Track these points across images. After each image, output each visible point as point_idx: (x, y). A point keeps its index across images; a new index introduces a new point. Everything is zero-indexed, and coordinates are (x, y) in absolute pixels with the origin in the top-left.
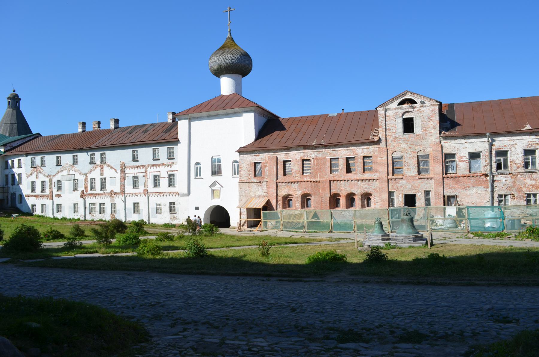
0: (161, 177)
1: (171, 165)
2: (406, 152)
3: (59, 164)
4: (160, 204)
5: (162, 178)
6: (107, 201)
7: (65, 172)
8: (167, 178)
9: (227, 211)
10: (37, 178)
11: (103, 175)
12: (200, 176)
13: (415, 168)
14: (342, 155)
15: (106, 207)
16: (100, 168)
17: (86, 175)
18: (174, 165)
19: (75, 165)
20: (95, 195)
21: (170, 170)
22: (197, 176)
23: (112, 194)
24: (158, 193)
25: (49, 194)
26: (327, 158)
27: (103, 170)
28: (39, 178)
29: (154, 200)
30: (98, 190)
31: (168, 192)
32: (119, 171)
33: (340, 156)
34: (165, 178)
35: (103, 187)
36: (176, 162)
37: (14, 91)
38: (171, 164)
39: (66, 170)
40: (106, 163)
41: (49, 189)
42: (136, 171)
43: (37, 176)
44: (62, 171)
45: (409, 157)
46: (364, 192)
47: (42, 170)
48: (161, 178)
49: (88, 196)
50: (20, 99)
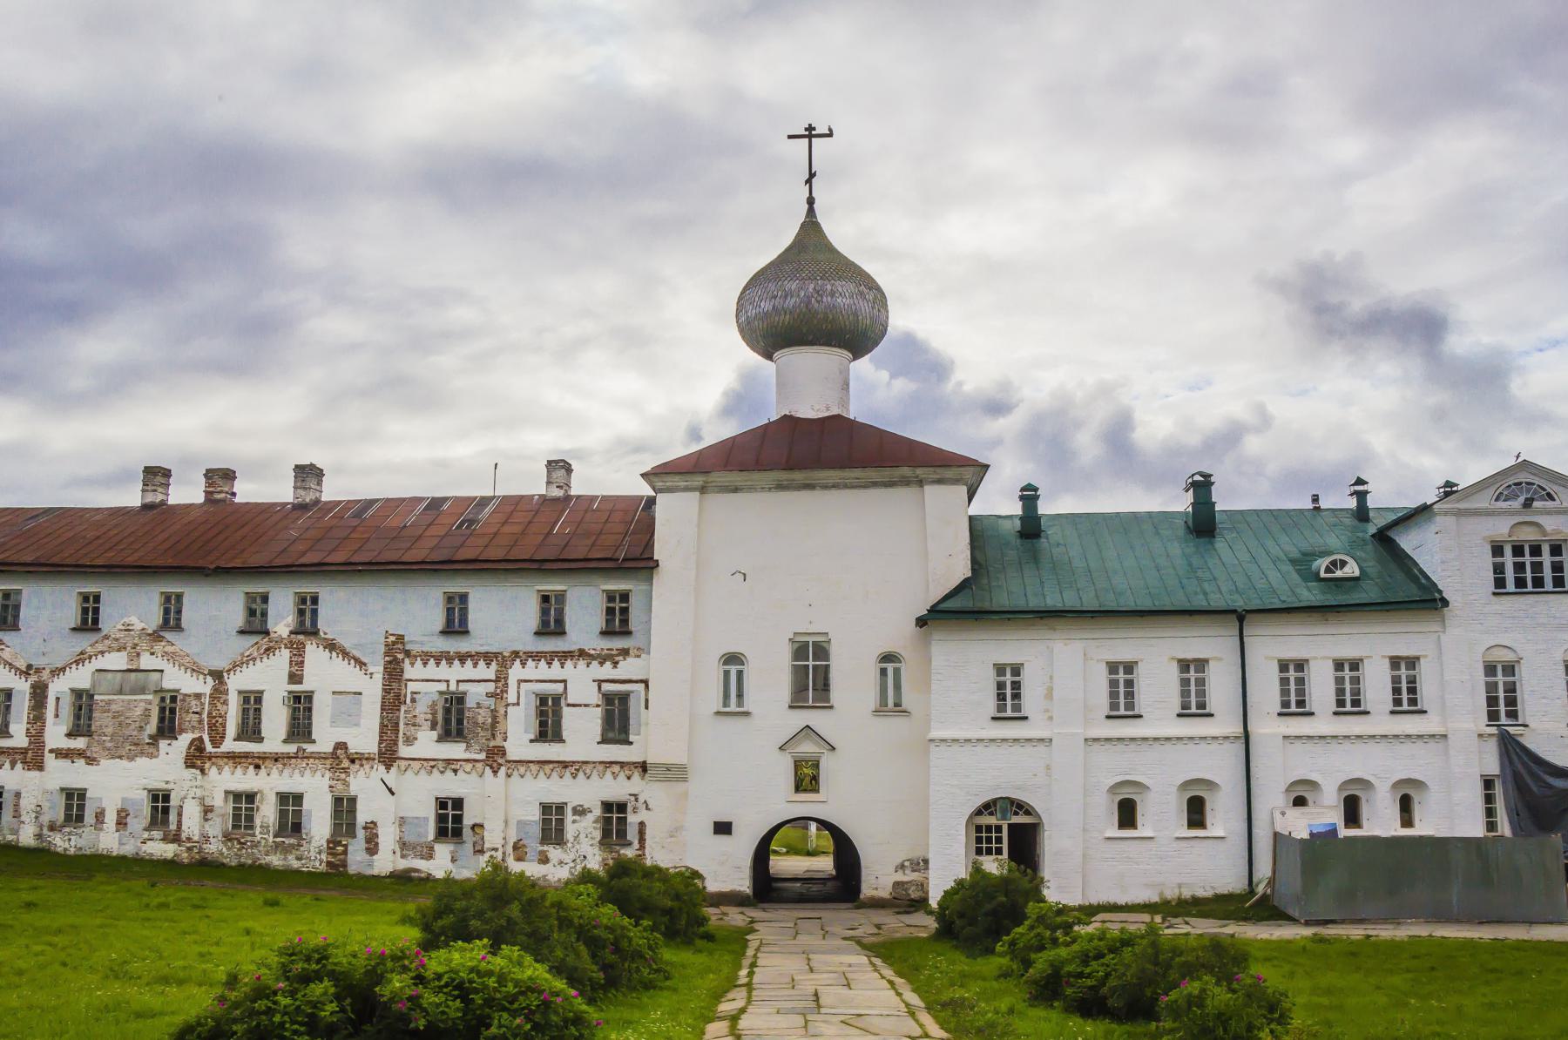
0: (570, 701)
1: (617, 658)
3: (89, 621)
4: (560, 808)
5: (574, 705)
7: (117, 661)
8: (598, 706)
11: (301, 683)
12: (740, 704)
15: (310, 812)
16: (288, 650)
17: (217, 675)
18: (630, 660)
19: (168, 635)
20: (257, 762)
21: (611, 677)
23: (341, 759)
27: (302, 662)
32: (378, 670)
34: (586, 706)
35: (300, 728)
36: (638, 649)
38: (617, 655)
39: (119, 650)
40: (314, 633)
41: (24, 726)
42: (454, 673)
48: (569, 705)
49: (221, 762)
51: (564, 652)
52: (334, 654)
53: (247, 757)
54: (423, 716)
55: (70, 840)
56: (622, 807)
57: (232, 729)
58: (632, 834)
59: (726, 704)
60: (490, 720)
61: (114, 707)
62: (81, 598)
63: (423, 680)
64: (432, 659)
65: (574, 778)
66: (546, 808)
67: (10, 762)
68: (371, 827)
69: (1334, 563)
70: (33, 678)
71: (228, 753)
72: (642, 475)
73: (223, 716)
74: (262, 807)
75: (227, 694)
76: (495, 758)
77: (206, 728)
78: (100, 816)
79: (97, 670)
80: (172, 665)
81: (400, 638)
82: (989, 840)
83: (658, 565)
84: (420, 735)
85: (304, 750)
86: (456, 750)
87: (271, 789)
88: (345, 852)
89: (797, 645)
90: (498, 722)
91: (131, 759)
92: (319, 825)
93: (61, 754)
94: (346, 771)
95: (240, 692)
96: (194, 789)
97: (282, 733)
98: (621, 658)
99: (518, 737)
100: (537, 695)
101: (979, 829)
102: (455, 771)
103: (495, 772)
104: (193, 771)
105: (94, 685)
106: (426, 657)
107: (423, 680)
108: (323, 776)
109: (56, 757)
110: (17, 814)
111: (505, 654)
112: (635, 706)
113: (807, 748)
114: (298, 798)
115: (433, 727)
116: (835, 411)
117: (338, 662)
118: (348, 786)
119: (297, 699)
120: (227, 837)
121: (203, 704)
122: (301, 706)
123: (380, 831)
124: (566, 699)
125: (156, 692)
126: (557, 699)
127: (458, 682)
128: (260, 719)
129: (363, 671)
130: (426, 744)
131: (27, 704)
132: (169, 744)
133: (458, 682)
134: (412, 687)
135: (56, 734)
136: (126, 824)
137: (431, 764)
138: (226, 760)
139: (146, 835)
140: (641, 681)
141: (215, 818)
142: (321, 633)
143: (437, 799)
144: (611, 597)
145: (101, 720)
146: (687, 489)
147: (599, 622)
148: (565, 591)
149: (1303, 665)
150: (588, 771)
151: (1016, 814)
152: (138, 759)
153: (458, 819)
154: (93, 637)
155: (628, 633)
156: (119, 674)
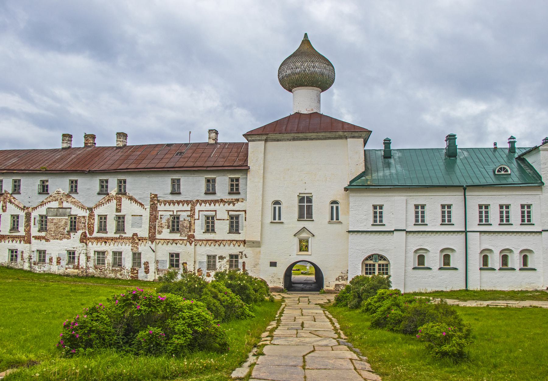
0: (217, 218)
3: (44, 189)
4: (214, 257)
6: (126, 250)
8: (228, 220)
9: (287, 269)
10: (4, 211)
11: (121, 212)
12: (280, 219)
15: (124, 258)
18: (239, 203)
19: (73, 195)
20: (106, 240)
22: (275, 219)
23: (135, 239)
24: (211, 240)
25: (24, 235)
27: (121, 204)
28: (7, 210)
29: (204, 251)
30: (111, 232)
31: (229, 240)
32: (148, 207)
34: (223, 220)
35: (120, 228)
39: (55, 201)
40: (125, 194)
41: (24, 228)
43: (4, 208)
44: (50, 202)
47: (14, 198)
48: (217, 219)
49: (93, 241)
51: (215, 200)
52: (132, 202)
53: (102, 239)
54: (164, 224)
55: (41, 268)
56: (236, 256)
57: (96, 229)
58: (240, 266)
59: (275, 219)
60: (189, 225)
61: (54, 221)
62: (42, 182)
63: (164, 211)
64: (167, 203)
65: (219, 246)
66: (209, 257)
67: (19, 241)
68: (146, 264)
69: (501, 168)
70: (26, 211)
71: (95, 237)
72: (243, 135)
73: (93, 224)
74: (108, 257)
75: (94, 216)
76: (191, 239)
77: (87, 228)
78: (51, 260)
79: (48, 208)
80: (74, 206)
81: (156, 196)
82: (370, 269)
83: (249, 168)
84: (163, 230)
85: (122, 236)
86: (177, 236)
87: (111, 250)
88: (137, 273)
89: (300, 198)
90: (192, 226)
91: (61, 240)
92: (128, 263)
93: (36, 238)
94: (137, 244)
95: (99, 216)
96: (83, 250)
97: (114, 230)
98: (236, 202)
99: (199, 232)
100: (206, 216)
101: (367, 265)
102: (176, 244)
103: (191, 244)
104: (83, 244)
105: (47, 213)
106: (165, 202)
107: (164, 211)
108: (129, 245)
109: (35, 239)
110: (22, 259)
111: (194, 201)
112: (241, 220)
113: (304, 235)
114: (120, 253)
115: (168, 228)
116: (315, 111)
117: (134, 204)
118: (138, 249)
119: (119, 218)
120: (96, 268)
121: (85, 220)
122: (120, 220)
123: (150, 265)
124: (216, 217)
125: (69, 216)
126: (213, 218)
127: (177, 211)
128: (106, 225)
129: (143, 208)
130: (166, 234)
131: (24, 220)
132: (74, 234)
133: (177, 211)
134: (160, 213)
135: (35, 231)
136: (60, 263)
137: (167, 241)
138: (94, 240)
139: (67, 266)
140: (243, 211)
141: (91, 261)
142: (127, 194)
143: (170, 253)
144: (232, 180)
145: (50, 226)
146: (259, 140)
147: (227, 189)
148: (216, 178)
149: (488, 206)
150: (224, 244)
151: (380, 260)
152: (63, 240)
153: (178, 261)
154: (46, 196)
155: (239, 193)
156: (56, 209)
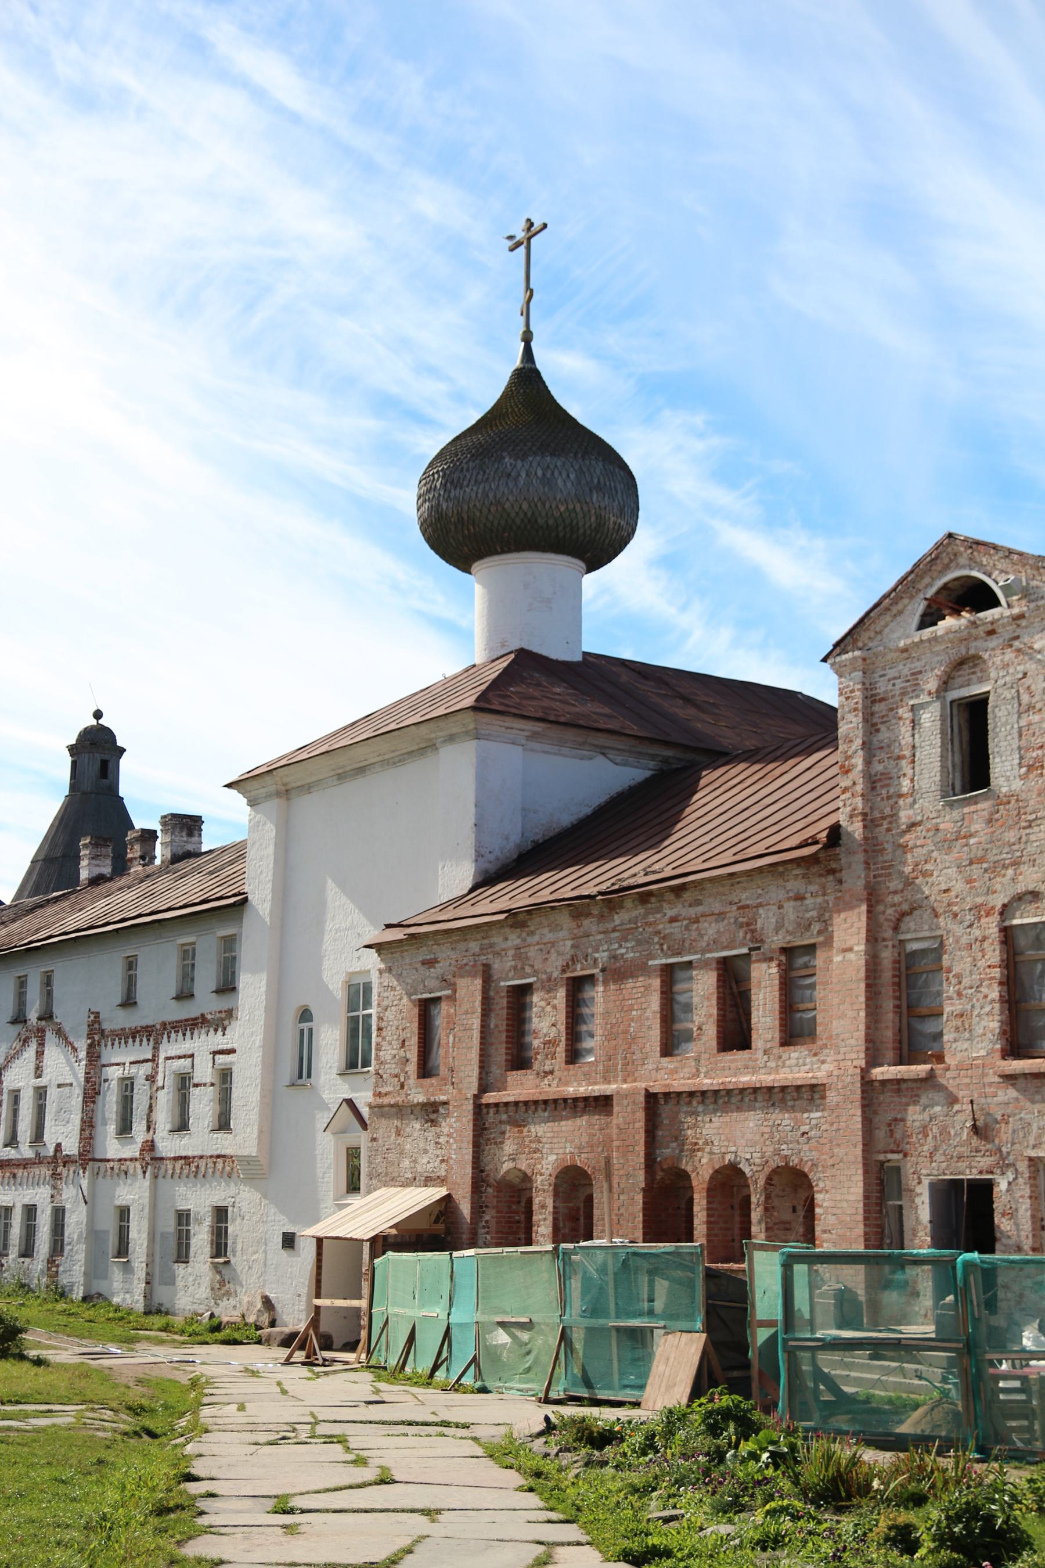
0: (196, 1081)
2: (955, 908)
8: (212, 1085)
13: (987, 1009)
14: (704, 944)
23: (58, 1160)
26: (650, 963)
33: (696, 953)
37: (98, 715)
45: (964, 940)
46: (776, 1162)
50: (122, 751)
148: (194, 943)
